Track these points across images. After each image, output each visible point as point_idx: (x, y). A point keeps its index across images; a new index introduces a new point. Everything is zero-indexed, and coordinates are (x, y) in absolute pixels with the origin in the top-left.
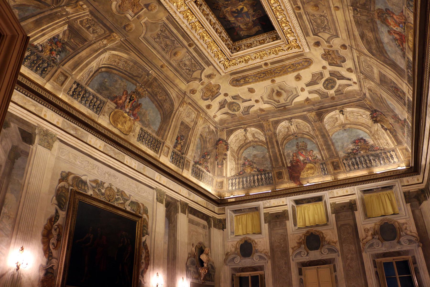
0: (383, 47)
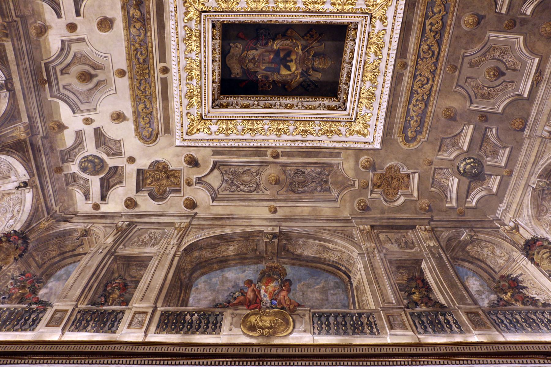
0: (212, 270)
